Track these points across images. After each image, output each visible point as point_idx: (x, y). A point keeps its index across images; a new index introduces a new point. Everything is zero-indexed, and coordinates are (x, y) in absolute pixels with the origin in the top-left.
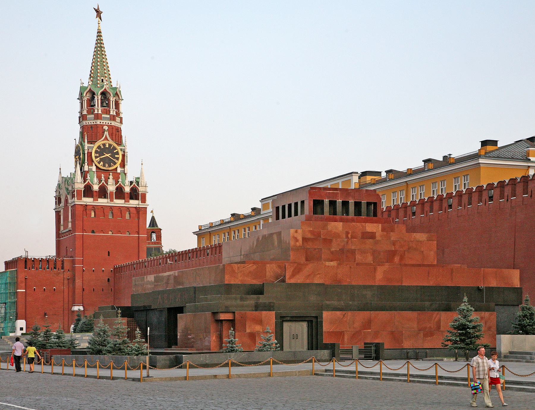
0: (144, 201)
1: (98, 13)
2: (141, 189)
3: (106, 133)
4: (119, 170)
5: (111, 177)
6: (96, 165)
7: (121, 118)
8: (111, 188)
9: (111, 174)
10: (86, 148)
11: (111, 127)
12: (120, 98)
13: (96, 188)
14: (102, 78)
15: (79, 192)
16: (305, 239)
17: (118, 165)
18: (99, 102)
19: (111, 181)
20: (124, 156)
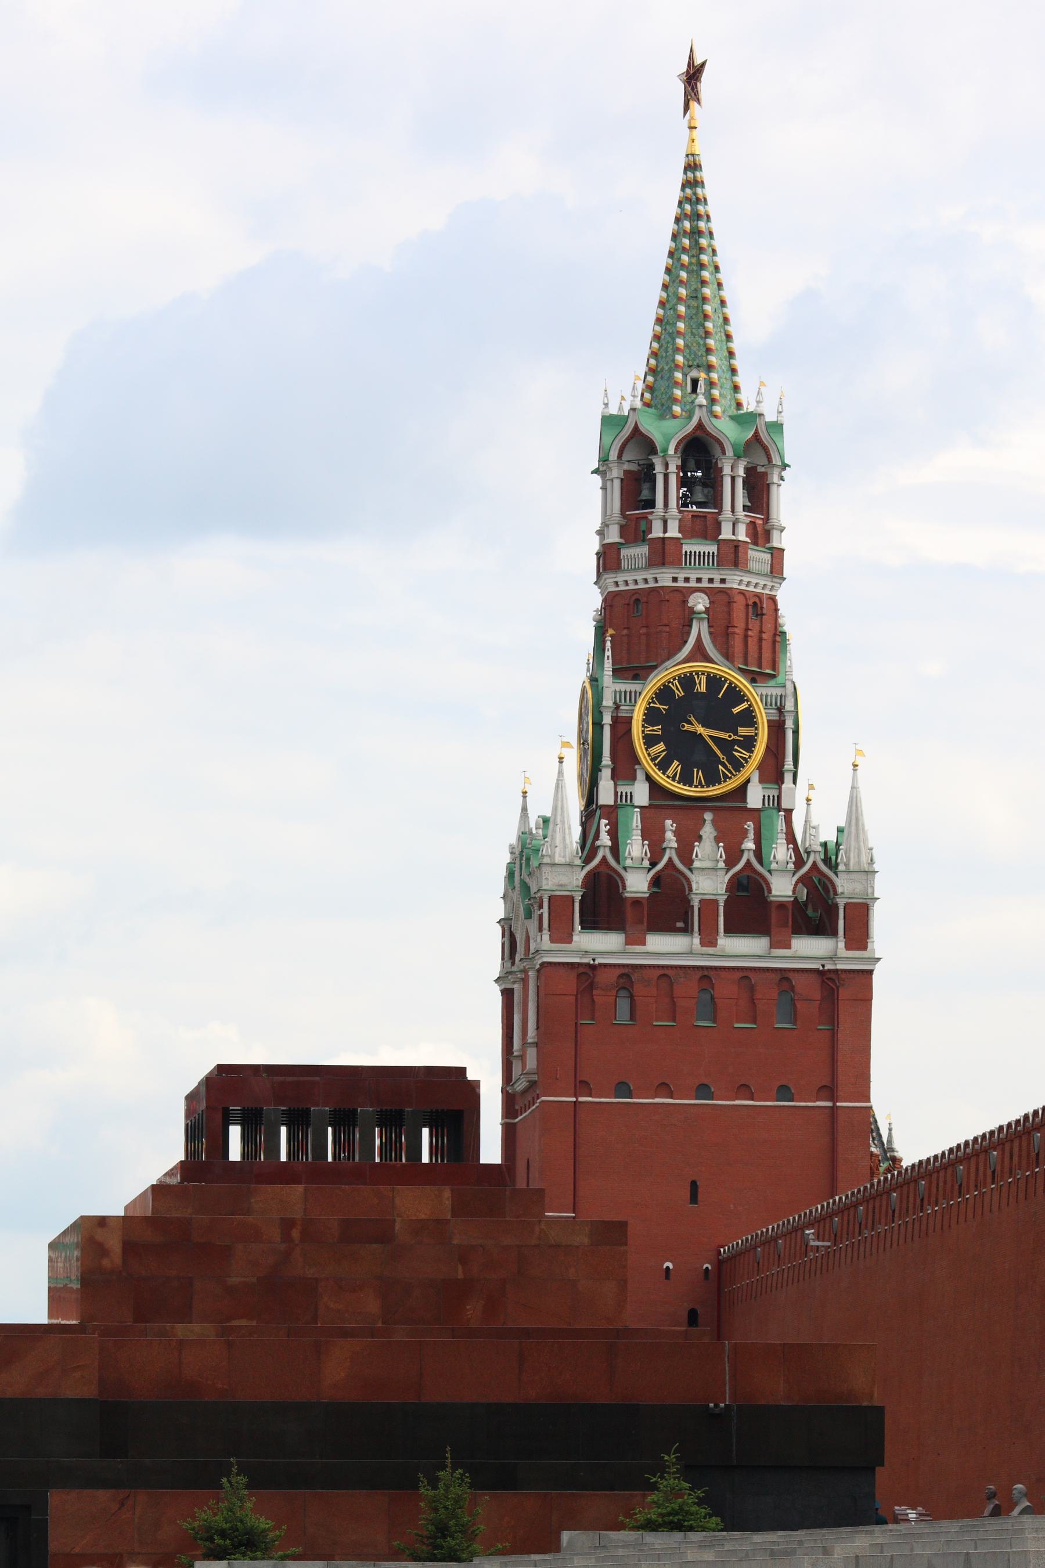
1: (693, 75)
2: (845, 886)
3: (699, 630)
4: (755, 797)
5: (708, 831)
6: (648, 778)
7: (777, 554)
8: (709, 882)
9: (708, 816)
10: (608, 702)
11: (722, 598)
12: (776, 460)
13: (637, 884)
14: (694, 373)
15: (559, 904)
16: (130, 1248)
17: (751, 770)
18: (688, 484)
19: (708, 850)
20: (777, 728)
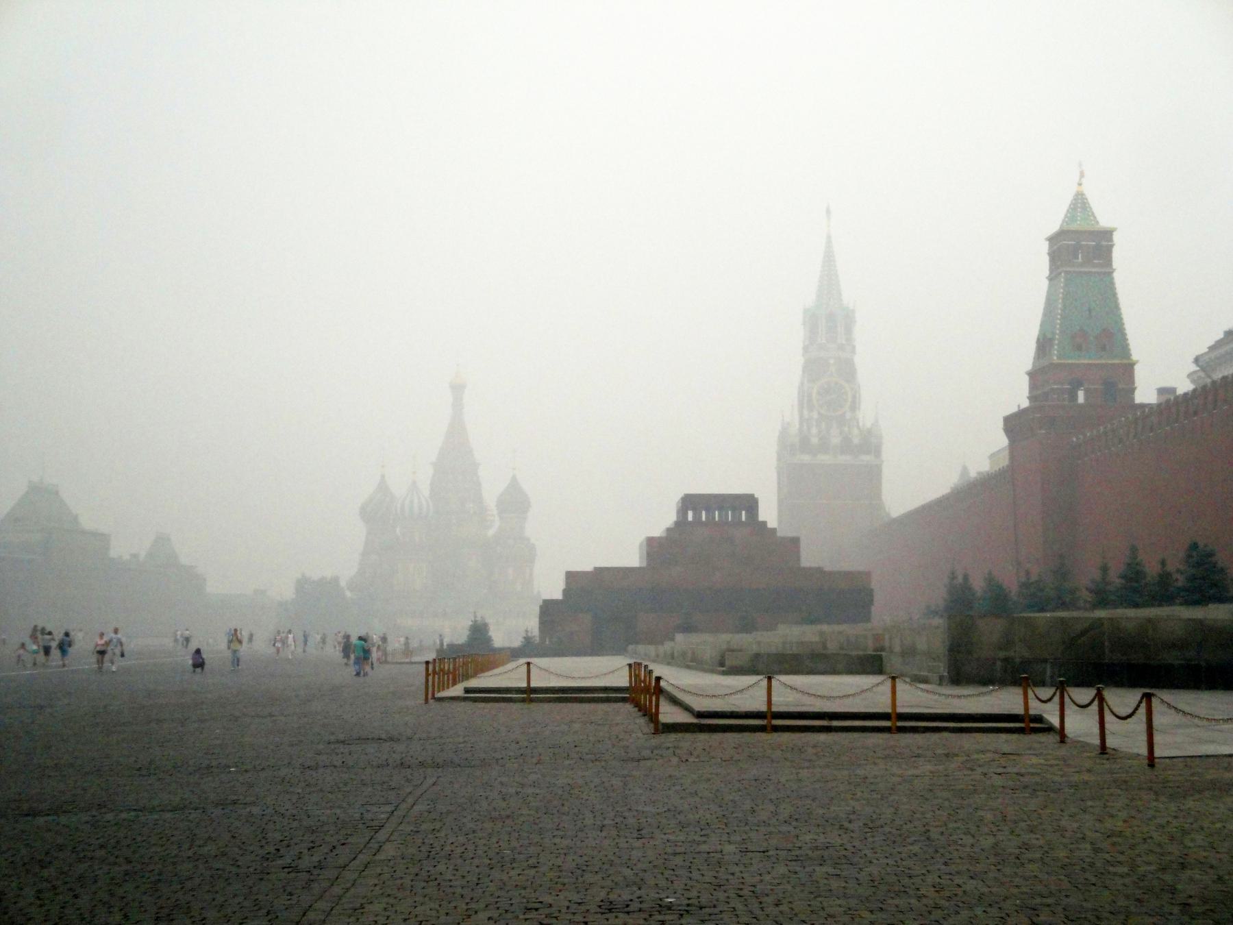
1: (828, 212)
4: (848, 416)
7: (854, 347)
8: (836, 440)
13: (815, 440)
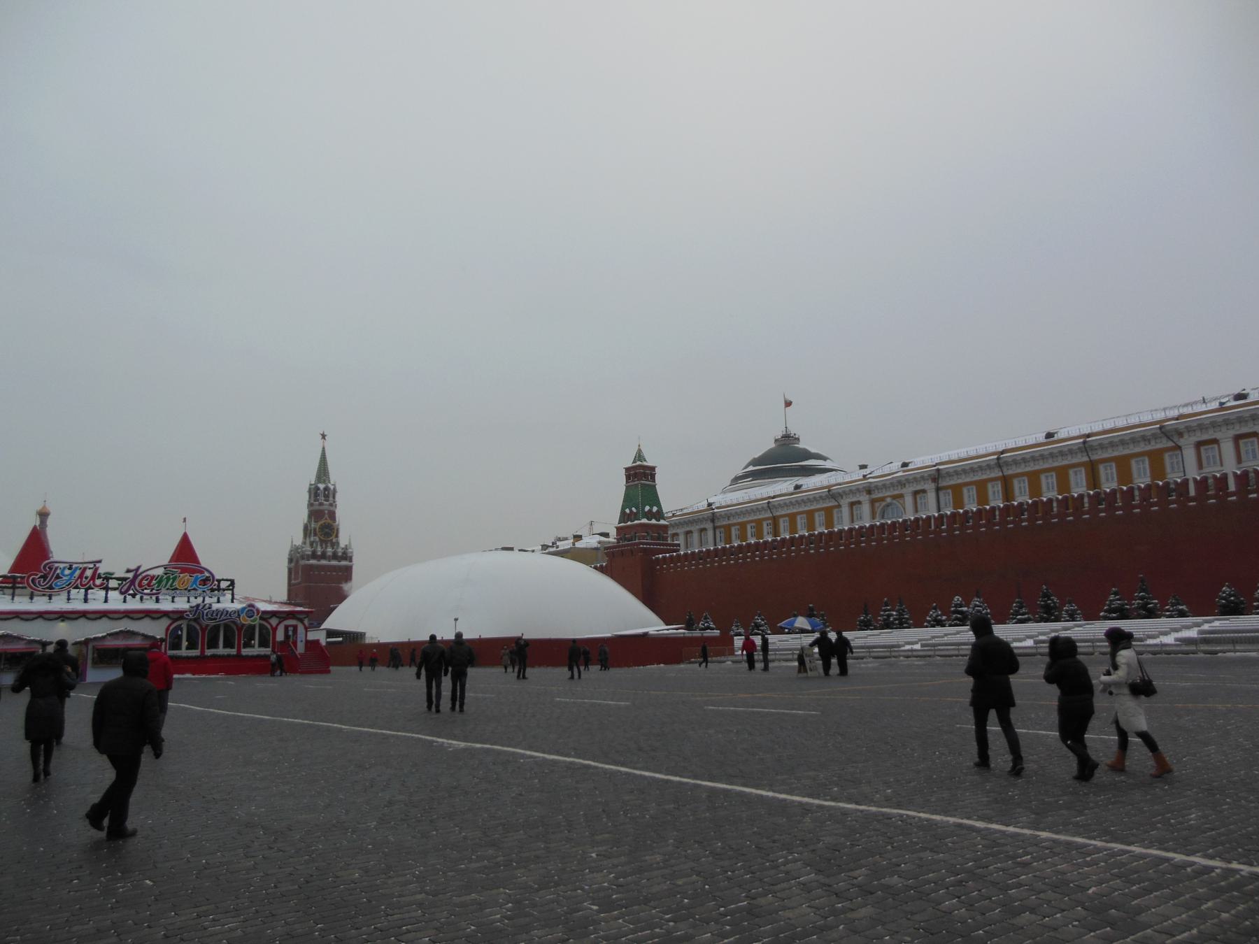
0: (351, 560)
1: (324, 436)
8: (330, 551)
